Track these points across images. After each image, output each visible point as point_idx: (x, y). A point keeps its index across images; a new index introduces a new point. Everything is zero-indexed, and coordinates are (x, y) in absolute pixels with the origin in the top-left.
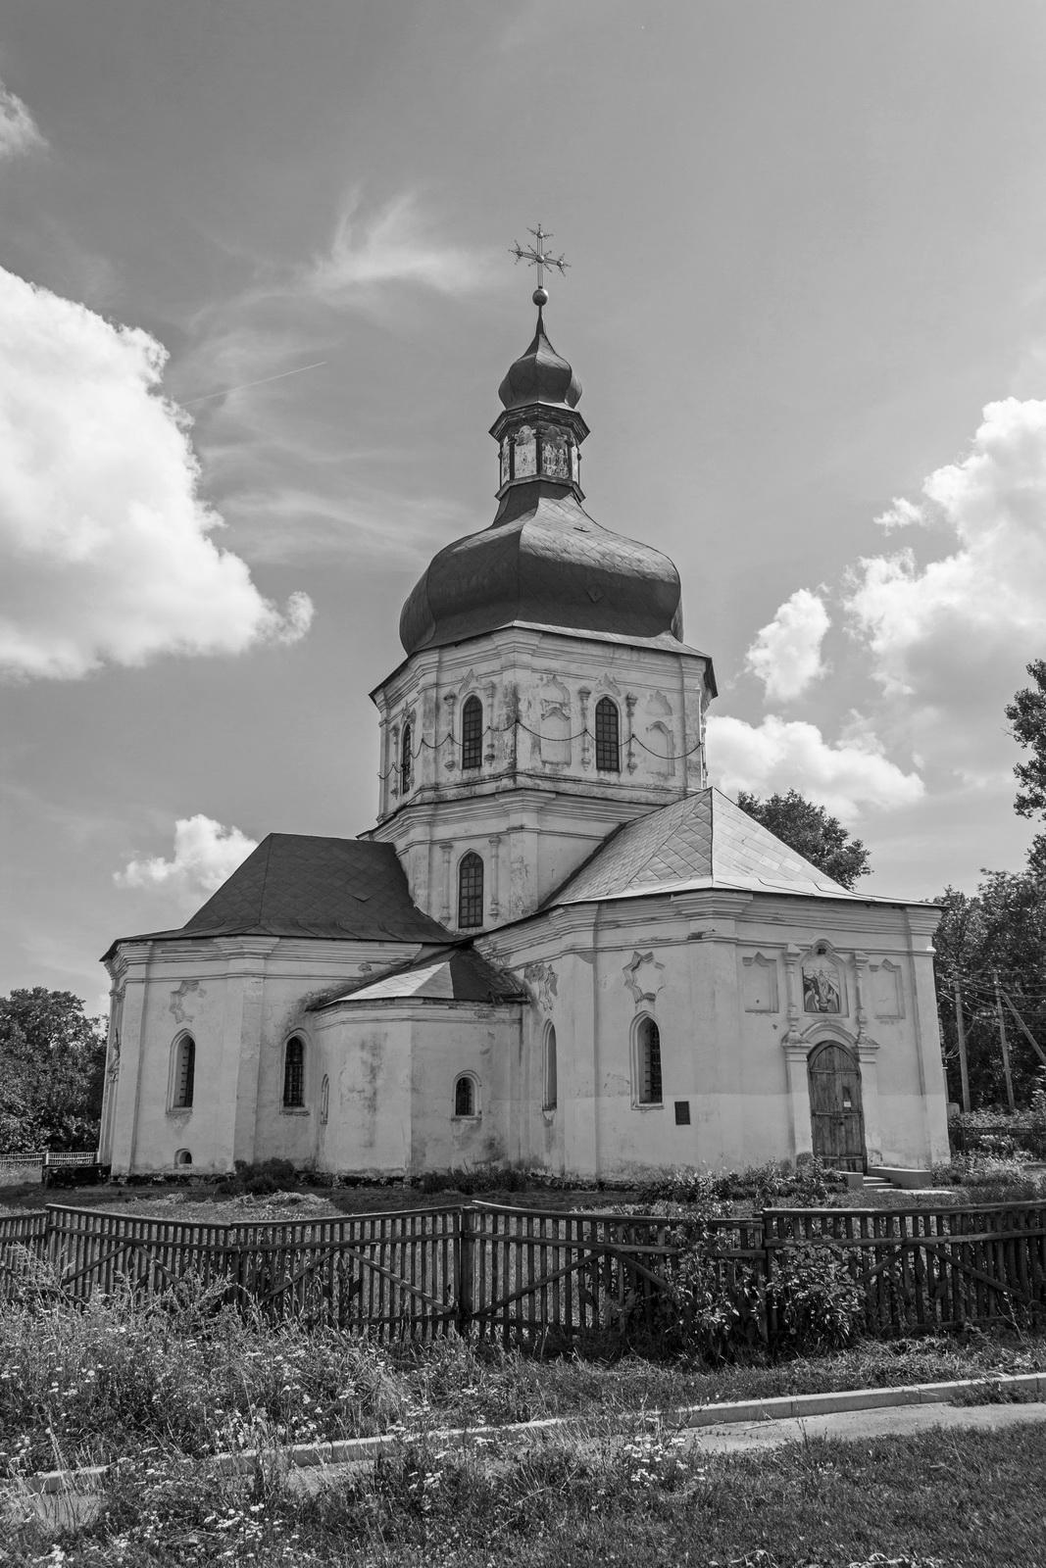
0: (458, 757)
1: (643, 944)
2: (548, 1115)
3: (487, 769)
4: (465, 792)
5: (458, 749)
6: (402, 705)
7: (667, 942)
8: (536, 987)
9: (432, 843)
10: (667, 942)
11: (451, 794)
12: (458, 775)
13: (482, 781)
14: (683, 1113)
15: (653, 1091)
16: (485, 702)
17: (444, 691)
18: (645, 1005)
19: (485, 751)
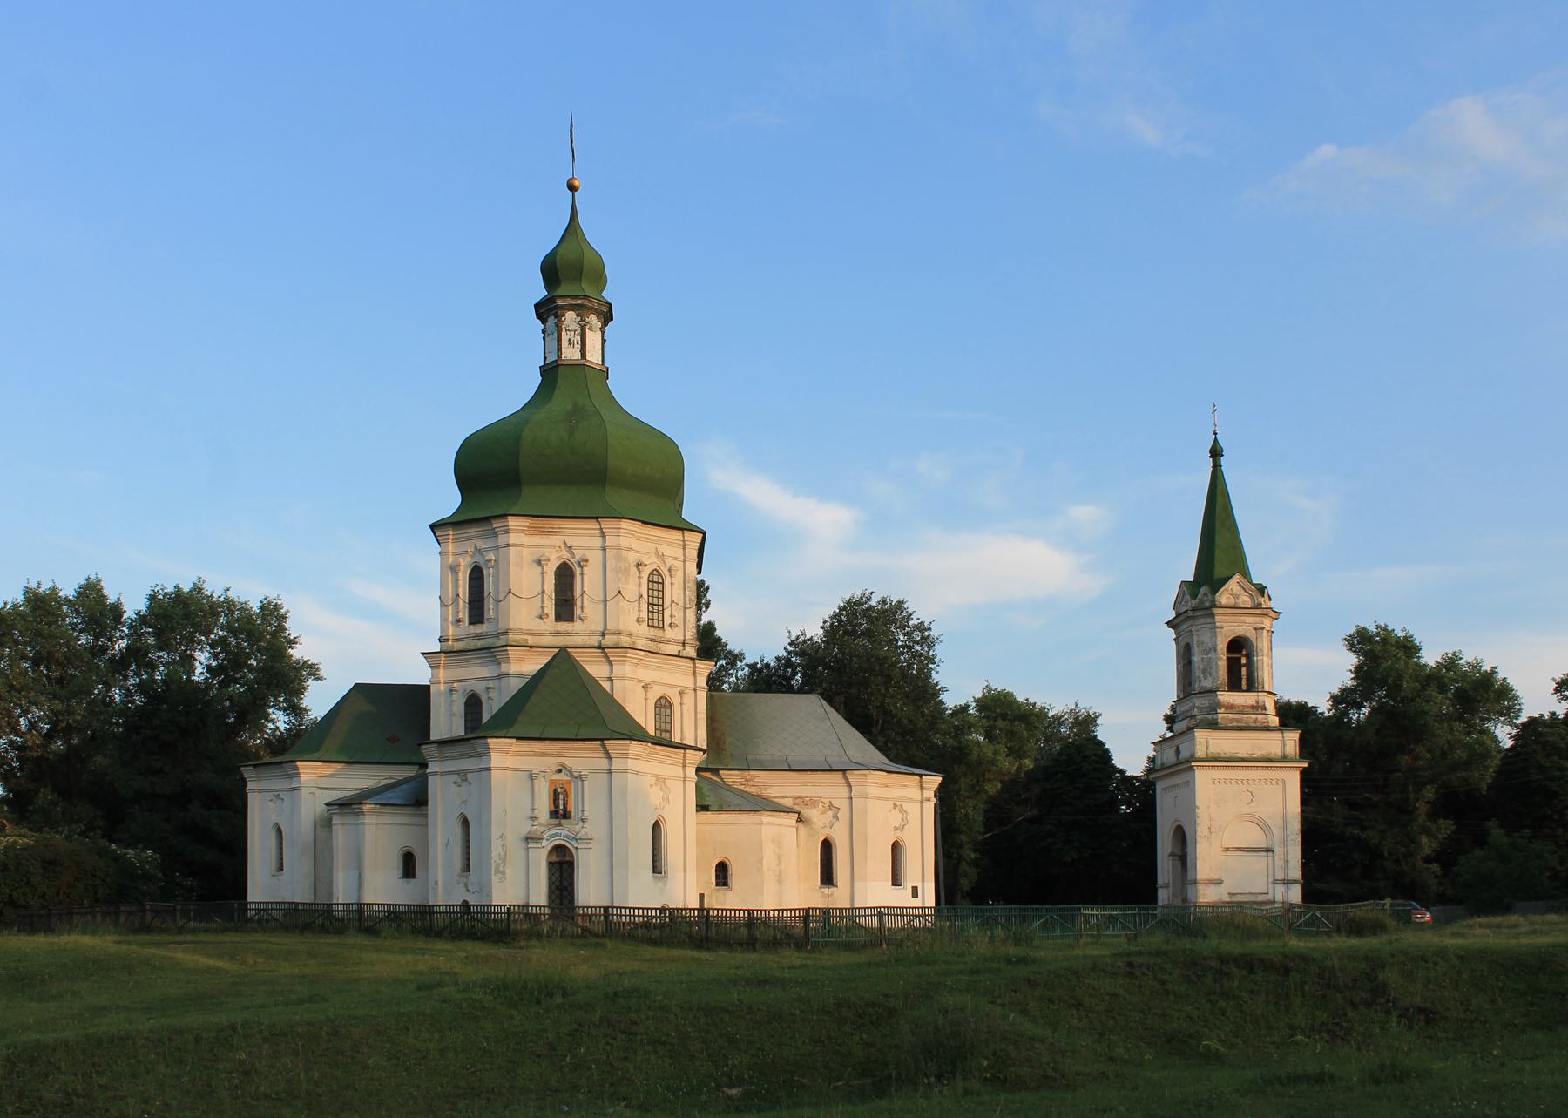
0: (644, 615)
1: (900, 799)
2: (825, 890)
3: (669, 634)
4: (653, 646)
5: (644, 606)
6: (556, 540)
7: (911, 800)
8: (811, 813)
9: (639, 681)
10: (911, 800)
11: (640, 644)
12: (644, 630)
13: (668, 642)
14: (915, 890)
15: (896, 881)
16: (668, 580)
17: (633, 557)
18: (898, 833)
19: (668, 621)
